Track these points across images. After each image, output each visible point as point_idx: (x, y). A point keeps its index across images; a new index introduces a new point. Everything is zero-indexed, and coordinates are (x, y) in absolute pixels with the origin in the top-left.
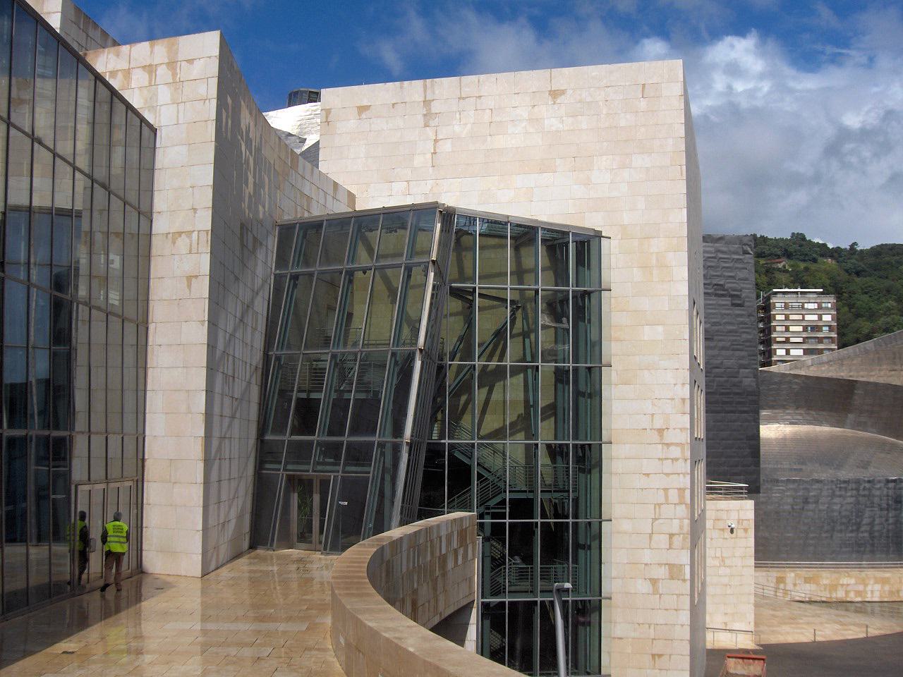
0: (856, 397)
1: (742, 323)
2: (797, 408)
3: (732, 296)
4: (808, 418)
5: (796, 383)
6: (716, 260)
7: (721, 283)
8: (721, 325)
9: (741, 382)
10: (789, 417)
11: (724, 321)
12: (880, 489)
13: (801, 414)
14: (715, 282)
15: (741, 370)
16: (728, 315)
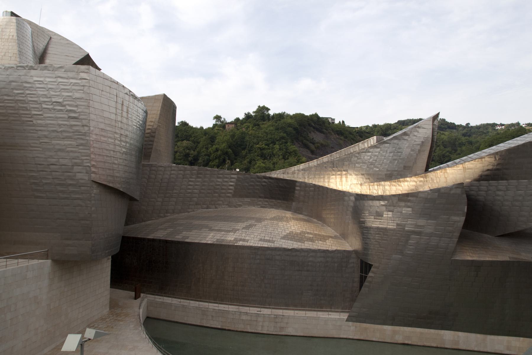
0: (296, 192)
1: (77, 131)
2: (265, 198)
3: (68, 111)
4: (271, 204)
5: (265, 182)
6: (56, 84)
7: (60, 100)
8: (58, 132)
9: (75, 176)
10: (260, 203)
11: (61, 129)
12: (279, 255)
13: (267, 201)
14: (54, 100)
15: (75, 167)
16: (64, 125)
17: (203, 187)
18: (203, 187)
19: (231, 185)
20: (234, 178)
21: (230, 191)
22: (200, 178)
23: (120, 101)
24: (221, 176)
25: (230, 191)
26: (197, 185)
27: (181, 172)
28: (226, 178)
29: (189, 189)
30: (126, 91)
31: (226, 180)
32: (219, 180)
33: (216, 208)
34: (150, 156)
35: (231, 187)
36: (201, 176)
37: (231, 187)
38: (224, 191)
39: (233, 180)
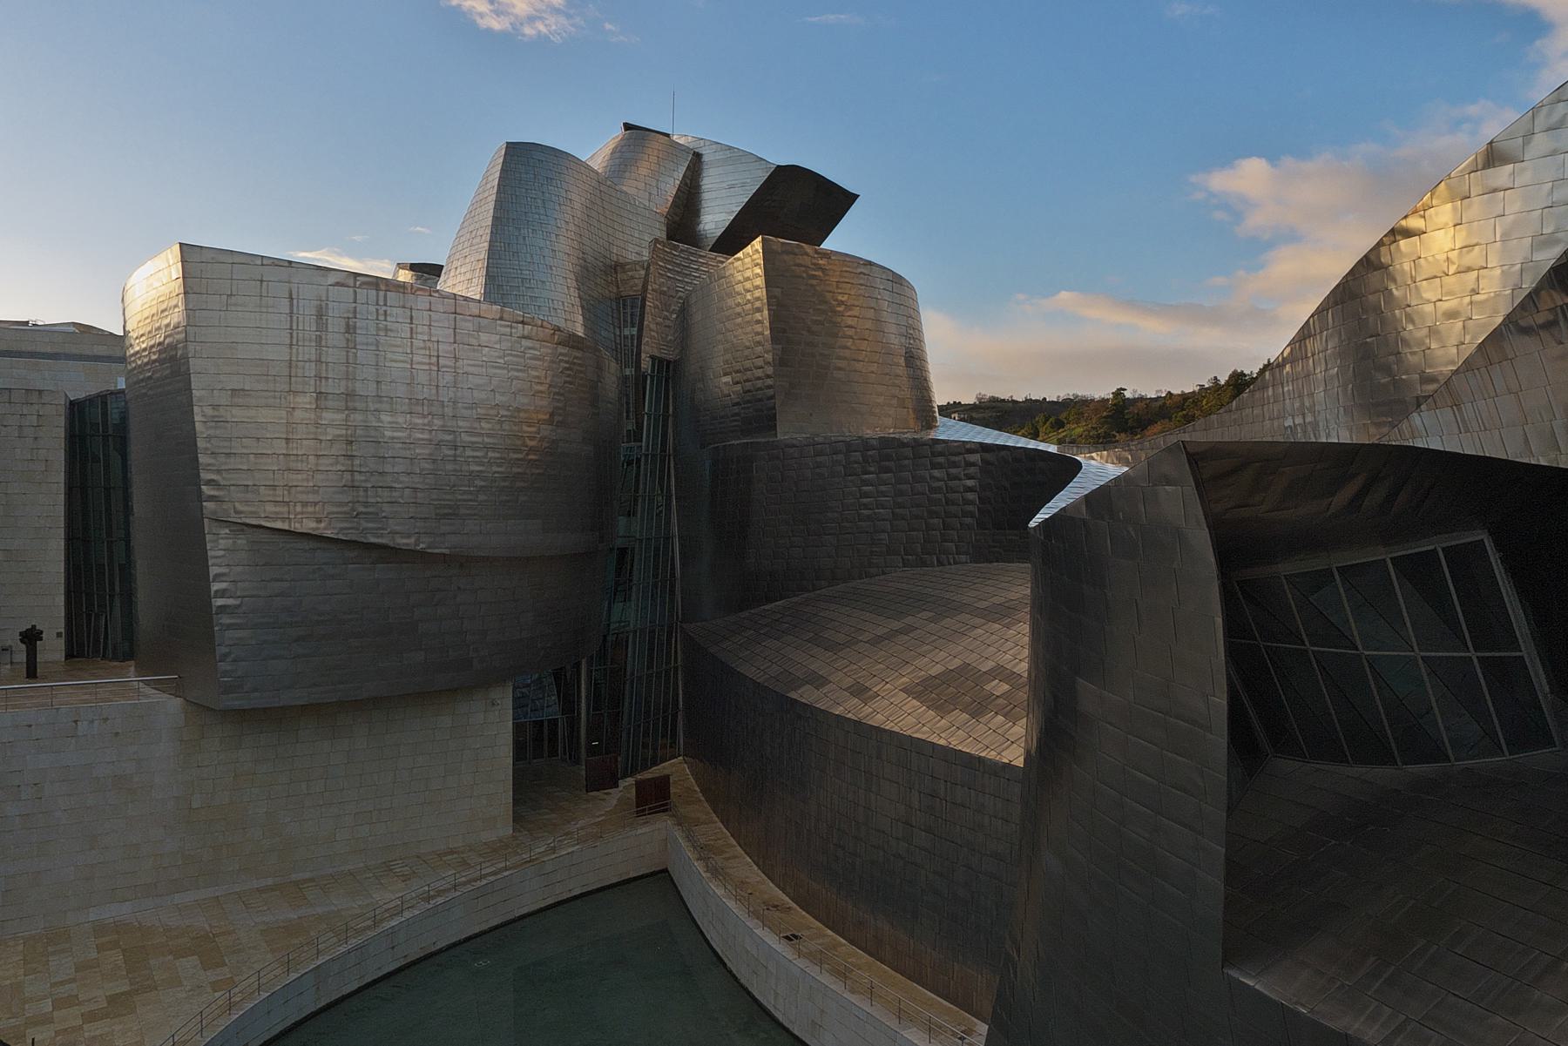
17: (900, 500)
18: (900, 500)
19: (970, 489)
20: (973, 464)
21: (970, 508)
22: (888, 470)
23: (307, 310)
24: (941, 460)
25: (970, 508)
26: (883, 494)
27: (840, 457)
28: (955, 465)
29: (866, 507)
30: (332, 279)
31: (953, 471)
32: (936, 473)
33: (940, 563)
34: (774, 418)
35: (971, 496)
36: (891, 464)
37: (971, 496)
38: (953, 509)
39: (972, 470)
